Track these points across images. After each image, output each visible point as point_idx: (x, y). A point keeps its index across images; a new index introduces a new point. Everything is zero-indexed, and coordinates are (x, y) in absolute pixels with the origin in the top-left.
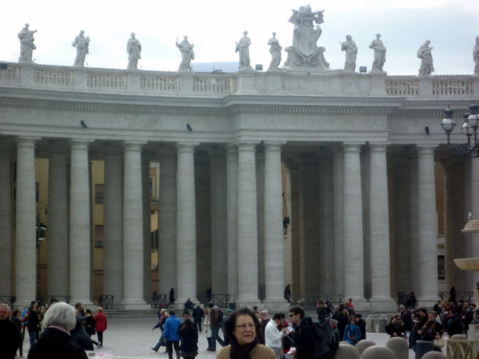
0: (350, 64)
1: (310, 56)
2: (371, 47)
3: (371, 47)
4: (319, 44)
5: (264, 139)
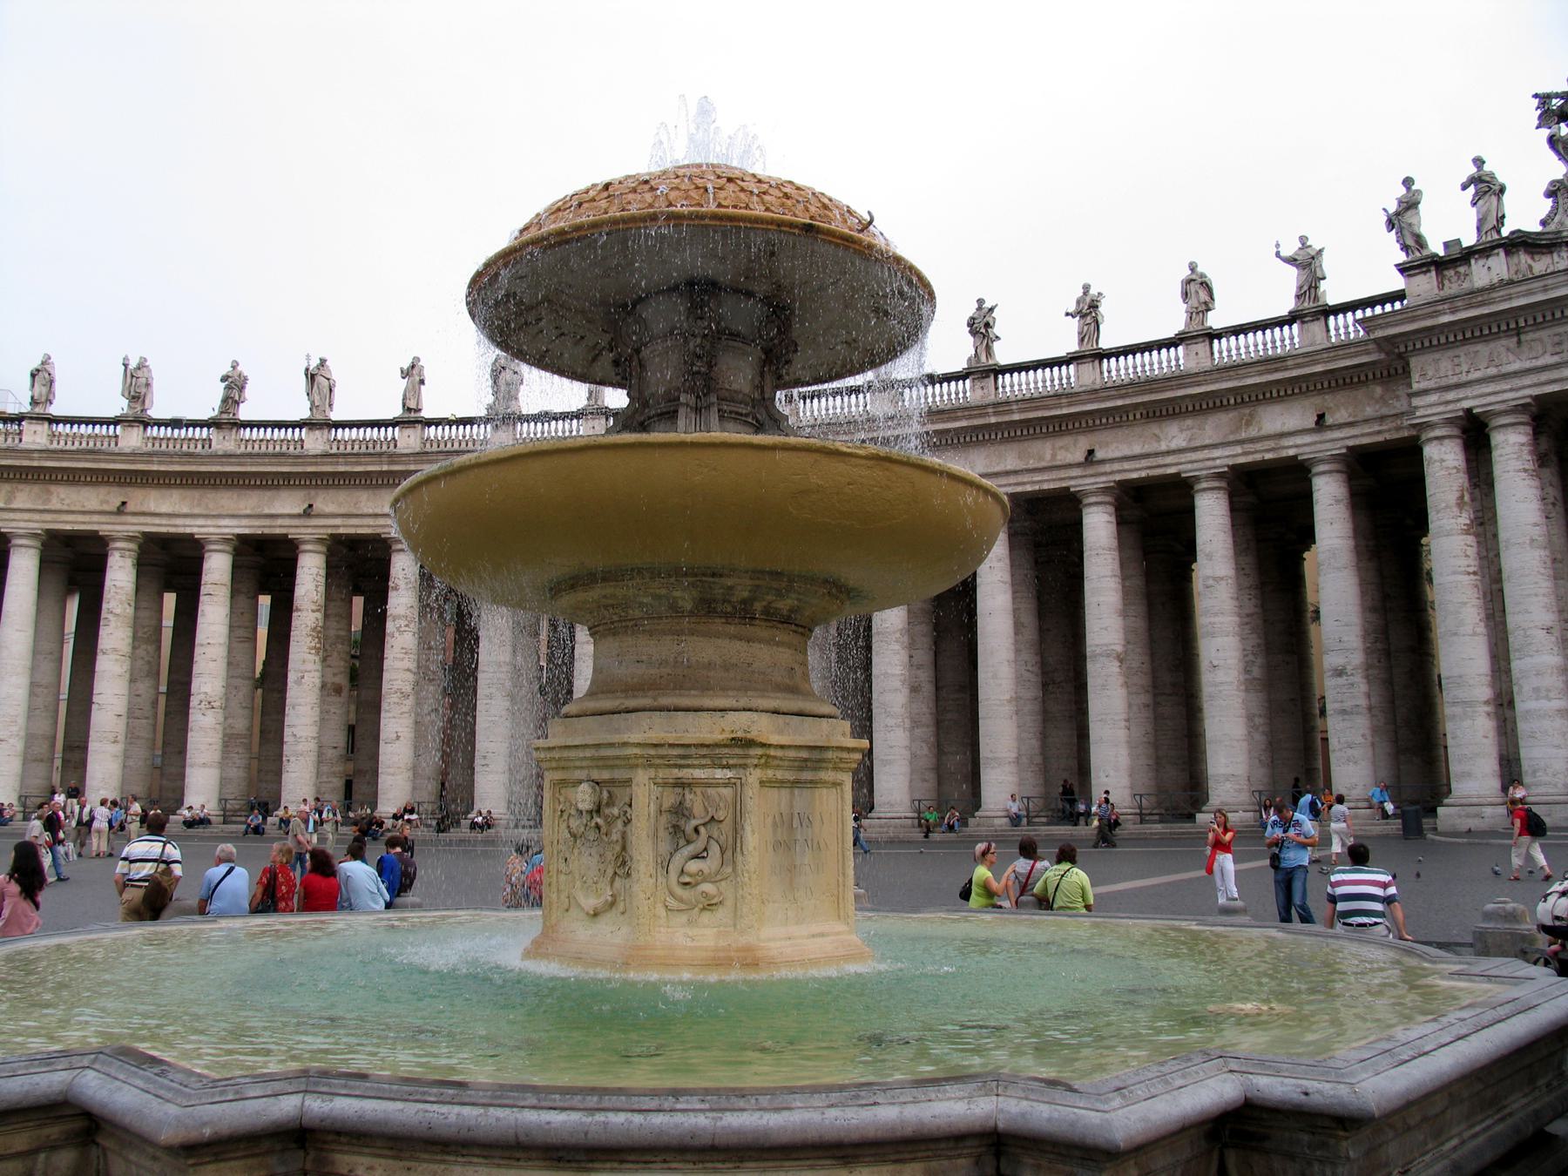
5: (1466, 404)
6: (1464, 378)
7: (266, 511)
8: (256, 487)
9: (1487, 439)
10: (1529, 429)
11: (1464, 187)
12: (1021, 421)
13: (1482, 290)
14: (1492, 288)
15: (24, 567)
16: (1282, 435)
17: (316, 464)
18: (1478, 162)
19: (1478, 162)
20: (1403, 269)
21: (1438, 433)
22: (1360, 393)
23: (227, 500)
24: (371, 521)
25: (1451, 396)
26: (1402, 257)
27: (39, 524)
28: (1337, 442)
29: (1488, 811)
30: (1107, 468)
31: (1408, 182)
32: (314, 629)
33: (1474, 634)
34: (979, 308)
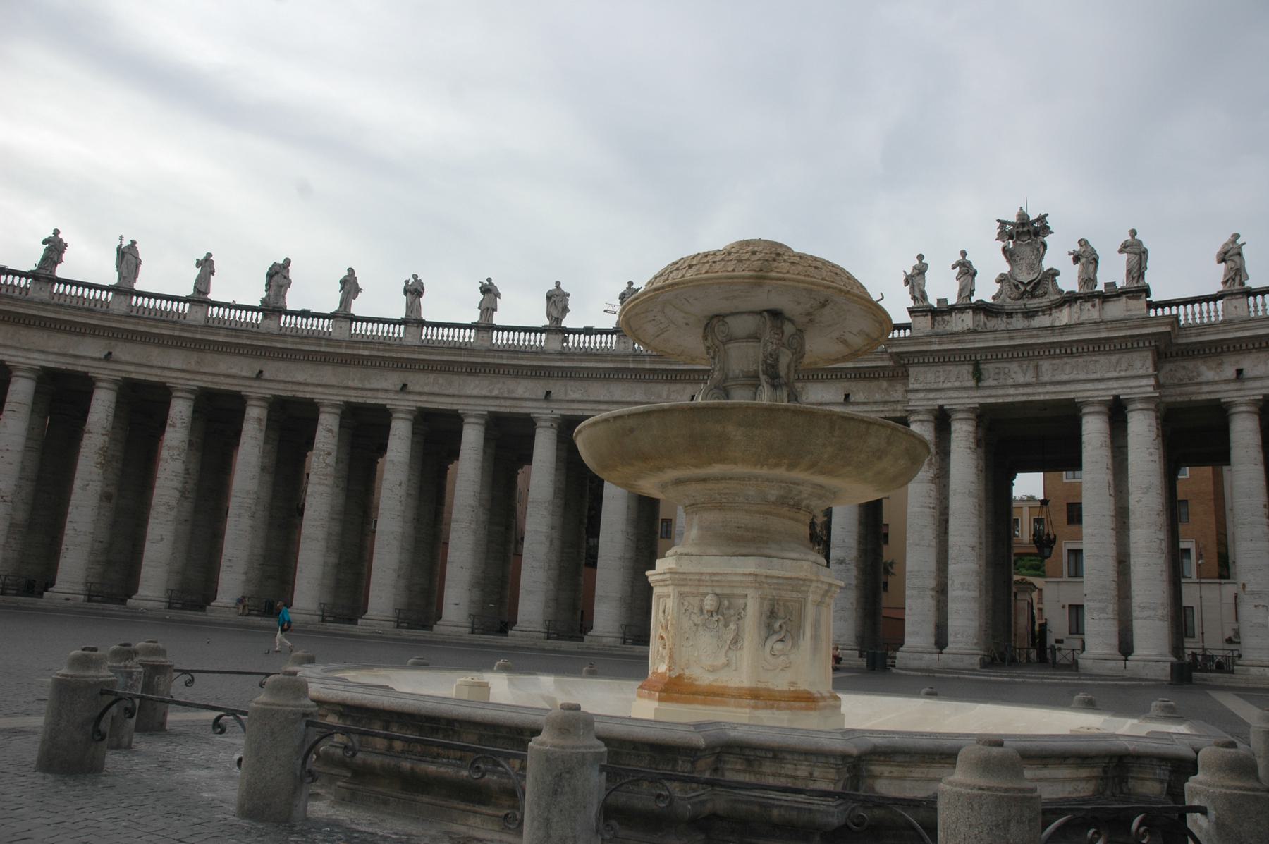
0: (1088, 280)
1: (1030, 283)
2: (1120, 251)
3: (1120, 251)
4: (1046, 264)
5: (940, 402)
6: (941, 386)
7: (71, 352)
8: (65, 331)
9: (949, 426)
10: (974, 423)
11: (954, 267)
12: (650, 370)
13: (957, 333)
14: (963, 333)
15: (21, 390)
17: (120, 322)
18: (964, 253)
19: (964, 253)
20: (912, 311)
21: (920, 417)
22: (873, 384)
23: (38, 338)
24: (159, 372)
25: (932, 395)
26: (911, 304)
27: (339, 397)
29: (927, 656)
31: (921, 257)
32: (101, 449)
33: (929, 546)
34: (629, 288)
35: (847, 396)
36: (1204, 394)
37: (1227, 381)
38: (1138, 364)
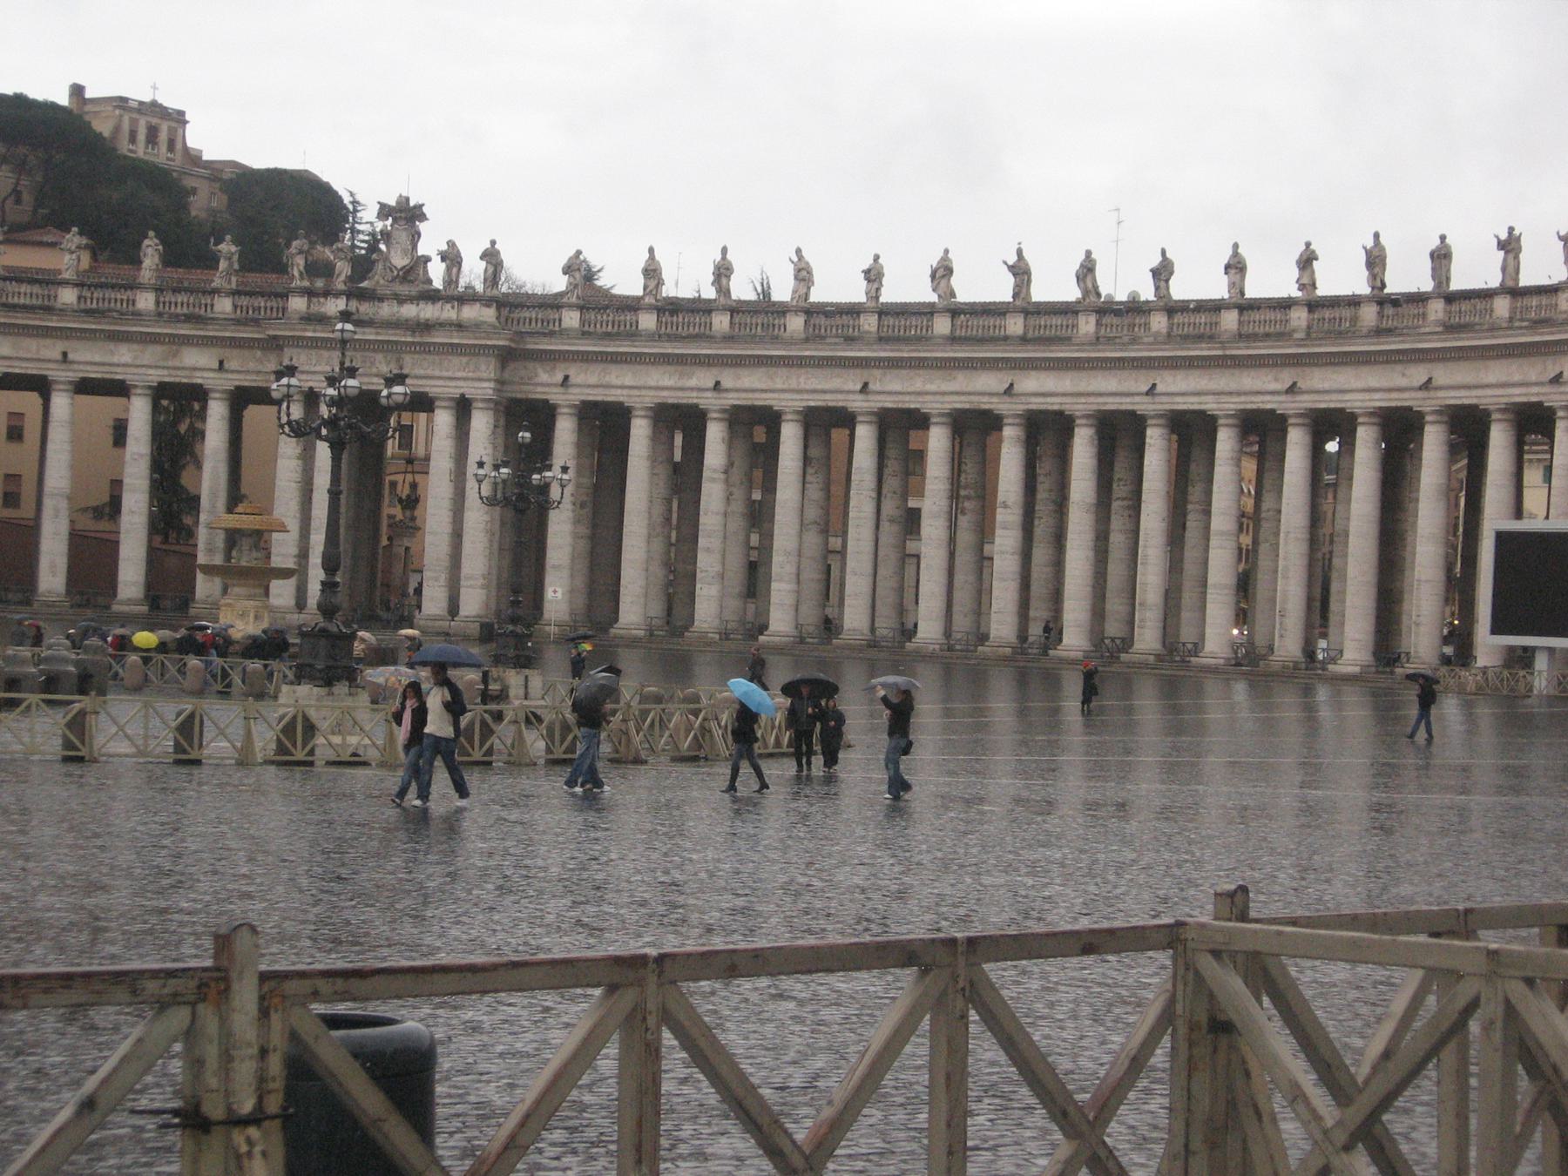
5: (311, 384)
16: (195, 369)
28: (230, 381)
30: (76, 367)
35: (221, 363)
36: (538, 393)
37: (555, 385)
38: (483, 367)
